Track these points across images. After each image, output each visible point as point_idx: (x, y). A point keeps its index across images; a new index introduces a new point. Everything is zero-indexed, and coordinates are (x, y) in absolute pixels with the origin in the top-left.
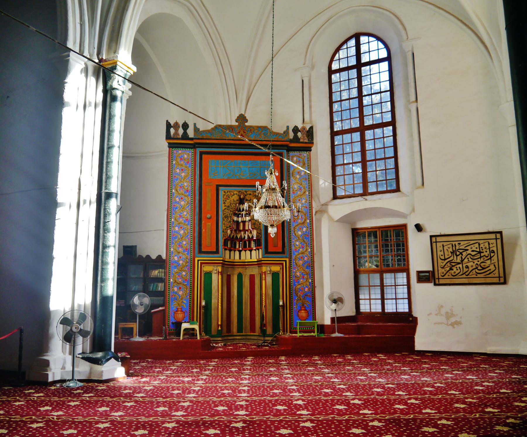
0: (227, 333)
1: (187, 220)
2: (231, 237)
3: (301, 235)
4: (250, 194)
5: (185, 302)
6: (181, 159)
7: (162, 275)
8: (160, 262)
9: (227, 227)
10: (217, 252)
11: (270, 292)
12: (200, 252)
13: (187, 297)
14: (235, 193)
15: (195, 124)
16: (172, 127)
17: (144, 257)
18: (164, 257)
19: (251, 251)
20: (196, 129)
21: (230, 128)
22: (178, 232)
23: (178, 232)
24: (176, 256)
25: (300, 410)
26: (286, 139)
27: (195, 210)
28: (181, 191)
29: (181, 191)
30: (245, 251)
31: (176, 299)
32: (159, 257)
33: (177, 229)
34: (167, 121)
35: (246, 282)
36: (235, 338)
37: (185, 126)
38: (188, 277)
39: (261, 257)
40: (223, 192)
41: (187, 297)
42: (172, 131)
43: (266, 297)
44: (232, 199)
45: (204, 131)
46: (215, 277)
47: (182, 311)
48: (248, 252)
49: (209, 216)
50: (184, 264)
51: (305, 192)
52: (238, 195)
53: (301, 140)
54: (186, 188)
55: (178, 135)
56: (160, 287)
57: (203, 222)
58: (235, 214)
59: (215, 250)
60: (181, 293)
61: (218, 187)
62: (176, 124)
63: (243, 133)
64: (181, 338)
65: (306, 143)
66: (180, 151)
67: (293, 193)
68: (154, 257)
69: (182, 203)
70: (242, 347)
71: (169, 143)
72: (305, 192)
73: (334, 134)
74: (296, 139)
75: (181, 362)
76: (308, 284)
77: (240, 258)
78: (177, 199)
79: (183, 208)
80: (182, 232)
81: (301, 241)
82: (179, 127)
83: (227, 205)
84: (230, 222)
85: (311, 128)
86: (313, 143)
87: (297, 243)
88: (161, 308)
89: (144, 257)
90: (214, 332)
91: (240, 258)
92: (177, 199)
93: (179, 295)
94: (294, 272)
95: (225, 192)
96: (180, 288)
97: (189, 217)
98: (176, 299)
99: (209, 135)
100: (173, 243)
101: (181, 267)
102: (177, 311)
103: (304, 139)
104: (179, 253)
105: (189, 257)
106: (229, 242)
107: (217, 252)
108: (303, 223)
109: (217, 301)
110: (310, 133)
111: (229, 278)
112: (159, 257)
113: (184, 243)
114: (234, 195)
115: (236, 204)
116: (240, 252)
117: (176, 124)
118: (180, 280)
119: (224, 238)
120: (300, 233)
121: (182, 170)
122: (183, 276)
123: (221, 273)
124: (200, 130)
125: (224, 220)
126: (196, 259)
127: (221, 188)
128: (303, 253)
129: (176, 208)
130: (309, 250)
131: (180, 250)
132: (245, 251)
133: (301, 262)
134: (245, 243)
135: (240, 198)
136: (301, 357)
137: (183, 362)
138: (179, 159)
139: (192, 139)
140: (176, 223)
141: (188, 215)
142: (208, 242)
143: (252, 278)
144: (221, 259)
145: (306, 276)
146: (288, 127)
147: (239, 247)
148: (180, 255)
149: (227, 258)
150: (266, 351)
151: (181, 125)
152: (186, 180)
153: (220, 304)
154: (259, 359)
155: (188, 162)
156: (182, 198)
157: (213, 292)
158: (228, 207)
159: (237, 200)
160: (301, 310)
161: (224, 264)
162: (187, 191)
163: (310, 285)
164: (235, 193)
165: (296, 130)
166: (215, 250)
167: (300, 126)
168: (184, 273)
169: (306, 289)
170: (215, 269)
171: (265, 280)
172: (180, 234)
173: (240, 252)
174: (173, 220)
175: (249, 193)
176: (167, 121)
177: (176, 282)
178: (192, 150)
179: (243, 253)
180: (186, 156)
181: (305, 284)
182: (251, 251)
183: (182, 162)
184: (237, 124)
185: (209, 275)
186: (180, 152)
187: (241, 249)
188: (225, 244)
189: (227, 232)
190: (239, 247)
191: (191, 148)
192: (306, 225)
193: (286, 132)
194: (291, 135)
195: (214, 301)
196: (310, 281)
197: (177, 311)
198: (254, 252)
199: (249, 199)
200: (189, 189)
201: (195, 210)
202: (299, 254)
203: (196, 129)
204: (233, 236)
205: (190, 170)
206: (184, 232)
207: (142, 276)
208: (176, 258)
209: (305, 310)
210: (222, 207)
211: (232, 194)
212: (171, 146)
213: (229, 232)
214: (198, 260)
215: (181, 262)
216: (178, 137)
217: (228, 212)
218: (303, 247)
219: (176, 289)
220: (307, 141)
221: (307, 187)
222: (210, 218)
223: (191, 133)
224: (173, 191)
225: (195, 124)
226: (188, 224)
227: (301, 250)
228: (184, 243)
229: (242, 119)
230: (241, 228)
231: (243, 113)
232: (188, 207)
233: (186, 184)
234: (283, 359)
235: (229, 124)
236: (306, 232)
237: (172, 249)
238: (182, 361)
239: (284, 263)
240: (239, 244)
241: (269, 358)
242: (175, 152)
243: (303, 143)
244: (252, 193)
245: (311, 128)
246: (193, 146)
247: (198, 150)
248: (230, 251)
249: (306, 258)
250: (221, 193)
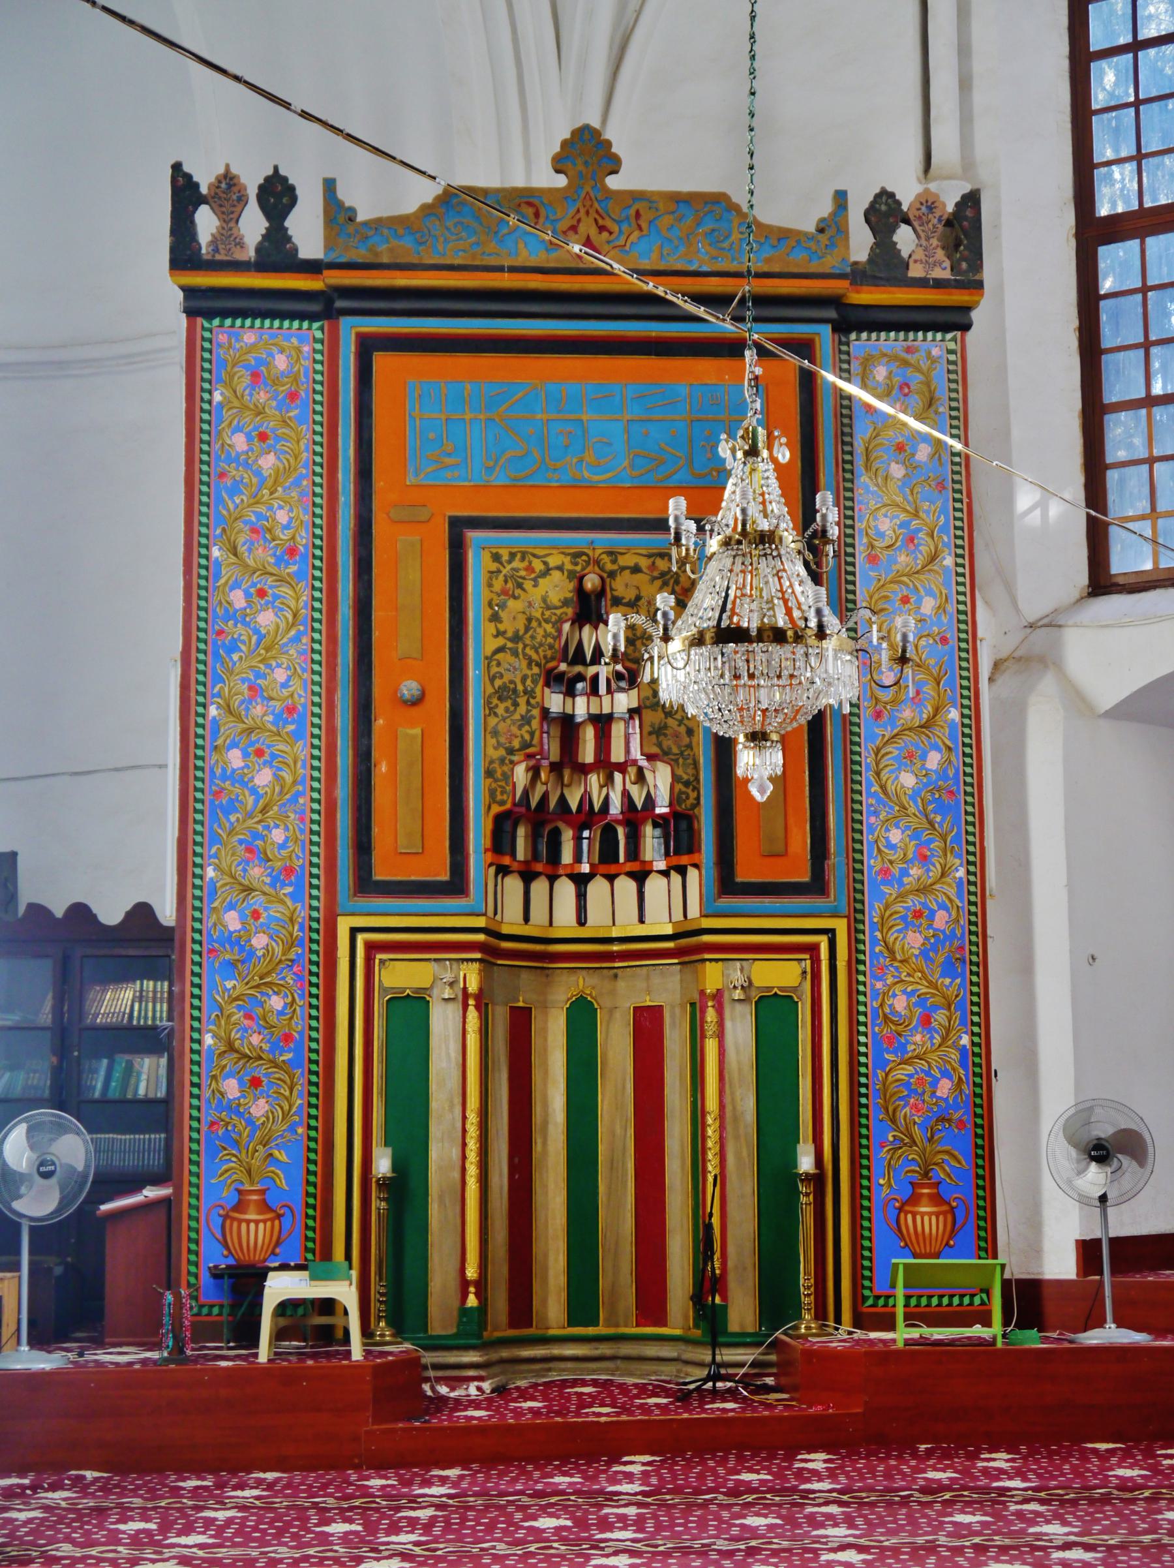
0: (512, 1324)
1: (291, 710)
2: (534, 803)
3: (916, 793)
4: (636, 570)
5: (282, 1156)
6: (256, 376)
7: (157, 1013)
8: (145, 944)
9: (511, 751)
10: (457, 885)
11: (746, 1103)
12: (365, 884)
13: (292, 1129)
14: (553, 561)
15: (330, 186)
16: (203, 200)
17: (59, 912)
18: (167, 914)
19: (640, 877)
20: (337, 214)
21: (527, 203)
22: (241, 779)
23: (241, 779)
24: (232, 907)
25: (1037, 1524)
26: (830, 263)
27: (332, 655)
28: (261, 555)
29: (261, 555)
30: (611, 878)
31: (236, 1144)
32: (142, 913)
33: (235, 759)
34: (177, 167)
36: (556, 1351)
37: (277, 195)
38: (298, 1026)
39: (694, 911)
40: (486, 556)
41: (292, 1129)
42: (206, 222)
43: (722, 1128)
44: (535, 594)
45: (377, 224)
46: (444, 1021)
47: (264, 1206)
48: (626, 886)
49: (409, 688)
50: (278, 950)
51: (933, 558)
52: (571, 575)
53: (916, 271)
54: (284, 536)
55: (241, 244)
56: (148, 1076)
57: (379, 723)
58: (553, 679)
59: (445, 877)
60: (259, 1108)
62: (228, 182)
63: (593, 232)
64: (264, 1354)
65: (939, 284)
66: (249, 335)
67: (873, 559)
68: (111, 914)
69: (266, 619)
70: (594, 1400)
71: (190, 292)
72: (933, 558)
73: (1093, 233)
74: (886, 265)
75: (259, 1483)
76: (955, 1056)
77: (581, 921)
78: (238, 599)
79: (267, 645)
80: (263, 778)
81: (914, 822)
82: (243, 200)
83: (507, 626)
84: (526, 720)
85: (971, 200)
86: (979, 285)
87: (895, 836)
88: (150, 1193)
89: (59, 912)
90: (440, 1321)
91: (581, 921)
92: (238, 599)
93: (250, 1122)
94: (876, 993)
95: (496, 558)
96: (256, 1082)
97: (299, 692)
98: (236, 1144)
99: (407, 247)
100: (216, 839)
101: (262, 967)
102: (240, 1207)
103: (930, 265)
104: (248, 890)
105: (302, 914)
106: (521, 832)
107: (457, 885)
108: (927, 725)
109: (456, 1153)
110: (963, 229)
111: (521, 1025)
112: (142, 913)
113: (278, 835)
114: (547, 572)
115: (561, 621)
117: (228, 182)
118: (255, 1039)
119: (496, 809)
120: (908, 780)
121: (263, 437)
122: (273, 1019)
123: (479, 997)
124: (361, 218)
125: (492, 711)
126: (344, 925)
127: (474, 536)
129: (233, 648)
130: (961, 873)
131: (256, 873)
132: (611, 878)
133: (914, 941)
134: (609, 834)
135: (580, 590)
136: (915, 1454)
137: (270, 1486)
138: (243, 380)
139: (313, 267)
140: (229, 729)
141: (296, 686)
142: (408, 833)
143: (648, 1026)
144: (481, 922)
145: (940, 1017)
146: (841, 198)
147: (578, 859)
148: (257, 901)
149: (511, 920)
150: (723, 1422)
151: (252, 192)
152: (282, 497)
153: (472, 1170)
154: (688, 1467)
155: (293, 396)
156: (262, 593)
157: (434, 1105)
158: (516, 638)
159: (565, 603)
160: (914, 1200)
161: (494, 949)
162: (292, 551)
163: (963, 1063)
164: (553, 561)
165: (885, 213)
166: (445, 877)
167: (907, 194)
168: (276, 1003)
169: (945, 1088)
170: (448, 976)
171: (721, 1036)
172: (254, 791)
174: (213, 711)
175: (627, 560)
176: (177, 167)
177: (231, 1048)
178: (316, 330)
179: (597, 889)
181: (933, 1057)
182: (640, 877)
183: (262, 397)
185: (412, 1008)
186: (249, 338)
187: (585, 868)
188: (501, 841)
189: (508, 777)
190: (578, 859)
191: (313, 317)
192: (942, 734)
193: (833, 228)
194: (860, 243)
195: (441, 1152)
196: (965, 1040)
197: (240, 1207)
198: (655, 886)
199: (630, 595)
200: (303, 540)
201: (332, 655)
202: (901, 896)
203: (337, 214)
204: (545, 797)
206: (278, 779)
207: (45, 1017)
208: (232, 921)
209: (937, 1199)
211: (538, 566)
212: (200, 305)
213: (521, 775)
214: (354, 931)
215: (259, 941)
216: (240, 256)
217: (515, 669)
219: (231, 1088)
220: (946, 274)
221: (944, 529)
222: (417, 702)
223: (307, 233)
224: (216, 552)
225: (330, 186)
226: (296, 736)
227: (915, 871)
228: (278, 835)
229: (587, 152)
230: (588, 754)
231: (595, 123)
232: (297, 639)
233: (282, 517)
234: (819, 1466)
235: (518, 181)
236: (942, 774)
237: (210, 873)
238: (270, 1476)
239: (823, 942)
240: (578, 839)
241: (741, 1459)
242: (222, 338)
243: (922, 283)
244: (644, 563)
245: (971, 200)
246: (325, 307)
247: (351, 328)
248: (528, 877)
249: (941, 919)
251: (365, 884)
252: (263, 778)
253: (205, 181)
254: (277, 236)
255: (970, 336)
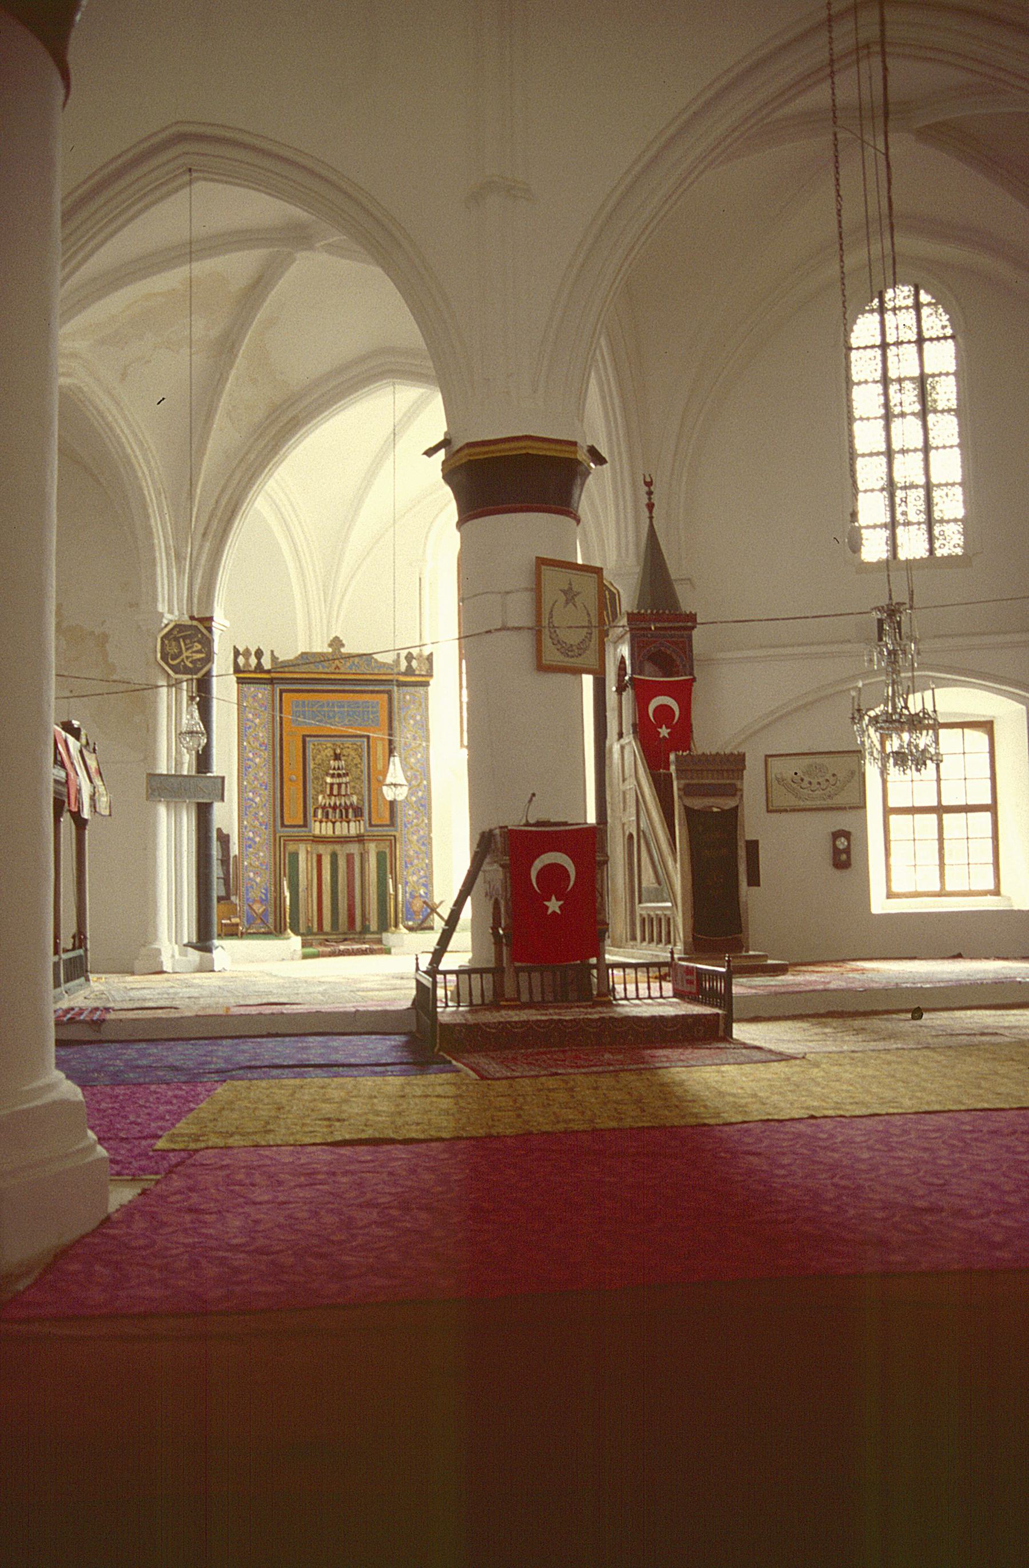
15: (272, 652)
19: (348, 822)
20: (274, 658)
33: (251, 794)
35: (342, 863)
37: (259, 654)
39: (362, 831)
44: (323, 753)
46: (302, 857)
48: (345, 824)
53: (417, 672)
60: (258, 880)
61: (304, 737)
65: (423, 676)
66: (252, 688)
71: (238, 678)
74: (410, 672)
85: (431, 654)
87: (411, 812)
108: (419, 785)
111: (319, 857)
113: (261, 814)
116: (334, 823)
126: (278, 835)
128: (417, 825)
131: (257, 823)
133: (415, 837)
135: (335, 754)
139: (268, 672)
143: (350, 858)
145: (421, 856)
167: (415, 652)
168: (261, 854)
173: (334, 823)
178: (269, 687)
179: (338, 824)
180: (260, 696)
182: (348, 822)
184: (330, 650)
193: (397, 662)
194: (404, 665)
198: (352, 824)
203: (274, 658)
205: (266, 716)
208: (251, 835)
210: (311, 765)
212: (240, 681)
218: (417, 818)
219: (252, 875)
223: (267, 664)
225: (272, 652)
229: (336, 643)
230: (335, 792)
243: (420, 675)
245: (431, 654)
246: (271, 681)
247: (278, 688)
248: (321, 822)
249: (422, 833)
250: (310, 747)
251: (283, 825)
252: (257, 800)
253: (241, 650)
254: (259, 664)
255: (430, 688)
